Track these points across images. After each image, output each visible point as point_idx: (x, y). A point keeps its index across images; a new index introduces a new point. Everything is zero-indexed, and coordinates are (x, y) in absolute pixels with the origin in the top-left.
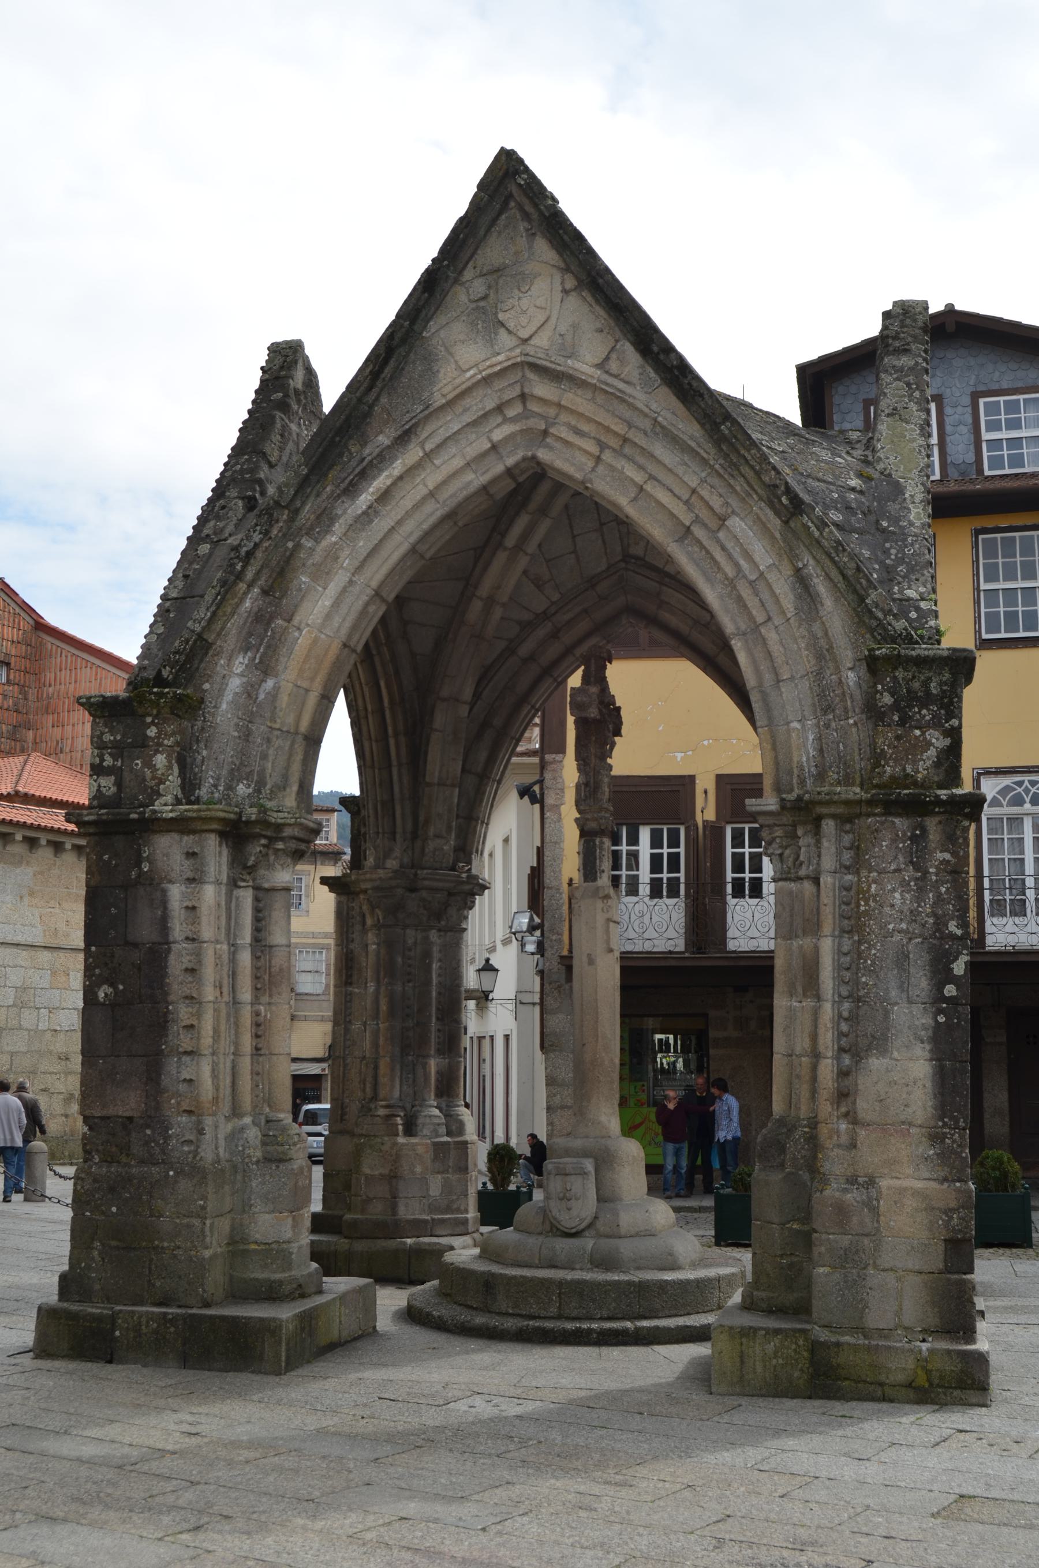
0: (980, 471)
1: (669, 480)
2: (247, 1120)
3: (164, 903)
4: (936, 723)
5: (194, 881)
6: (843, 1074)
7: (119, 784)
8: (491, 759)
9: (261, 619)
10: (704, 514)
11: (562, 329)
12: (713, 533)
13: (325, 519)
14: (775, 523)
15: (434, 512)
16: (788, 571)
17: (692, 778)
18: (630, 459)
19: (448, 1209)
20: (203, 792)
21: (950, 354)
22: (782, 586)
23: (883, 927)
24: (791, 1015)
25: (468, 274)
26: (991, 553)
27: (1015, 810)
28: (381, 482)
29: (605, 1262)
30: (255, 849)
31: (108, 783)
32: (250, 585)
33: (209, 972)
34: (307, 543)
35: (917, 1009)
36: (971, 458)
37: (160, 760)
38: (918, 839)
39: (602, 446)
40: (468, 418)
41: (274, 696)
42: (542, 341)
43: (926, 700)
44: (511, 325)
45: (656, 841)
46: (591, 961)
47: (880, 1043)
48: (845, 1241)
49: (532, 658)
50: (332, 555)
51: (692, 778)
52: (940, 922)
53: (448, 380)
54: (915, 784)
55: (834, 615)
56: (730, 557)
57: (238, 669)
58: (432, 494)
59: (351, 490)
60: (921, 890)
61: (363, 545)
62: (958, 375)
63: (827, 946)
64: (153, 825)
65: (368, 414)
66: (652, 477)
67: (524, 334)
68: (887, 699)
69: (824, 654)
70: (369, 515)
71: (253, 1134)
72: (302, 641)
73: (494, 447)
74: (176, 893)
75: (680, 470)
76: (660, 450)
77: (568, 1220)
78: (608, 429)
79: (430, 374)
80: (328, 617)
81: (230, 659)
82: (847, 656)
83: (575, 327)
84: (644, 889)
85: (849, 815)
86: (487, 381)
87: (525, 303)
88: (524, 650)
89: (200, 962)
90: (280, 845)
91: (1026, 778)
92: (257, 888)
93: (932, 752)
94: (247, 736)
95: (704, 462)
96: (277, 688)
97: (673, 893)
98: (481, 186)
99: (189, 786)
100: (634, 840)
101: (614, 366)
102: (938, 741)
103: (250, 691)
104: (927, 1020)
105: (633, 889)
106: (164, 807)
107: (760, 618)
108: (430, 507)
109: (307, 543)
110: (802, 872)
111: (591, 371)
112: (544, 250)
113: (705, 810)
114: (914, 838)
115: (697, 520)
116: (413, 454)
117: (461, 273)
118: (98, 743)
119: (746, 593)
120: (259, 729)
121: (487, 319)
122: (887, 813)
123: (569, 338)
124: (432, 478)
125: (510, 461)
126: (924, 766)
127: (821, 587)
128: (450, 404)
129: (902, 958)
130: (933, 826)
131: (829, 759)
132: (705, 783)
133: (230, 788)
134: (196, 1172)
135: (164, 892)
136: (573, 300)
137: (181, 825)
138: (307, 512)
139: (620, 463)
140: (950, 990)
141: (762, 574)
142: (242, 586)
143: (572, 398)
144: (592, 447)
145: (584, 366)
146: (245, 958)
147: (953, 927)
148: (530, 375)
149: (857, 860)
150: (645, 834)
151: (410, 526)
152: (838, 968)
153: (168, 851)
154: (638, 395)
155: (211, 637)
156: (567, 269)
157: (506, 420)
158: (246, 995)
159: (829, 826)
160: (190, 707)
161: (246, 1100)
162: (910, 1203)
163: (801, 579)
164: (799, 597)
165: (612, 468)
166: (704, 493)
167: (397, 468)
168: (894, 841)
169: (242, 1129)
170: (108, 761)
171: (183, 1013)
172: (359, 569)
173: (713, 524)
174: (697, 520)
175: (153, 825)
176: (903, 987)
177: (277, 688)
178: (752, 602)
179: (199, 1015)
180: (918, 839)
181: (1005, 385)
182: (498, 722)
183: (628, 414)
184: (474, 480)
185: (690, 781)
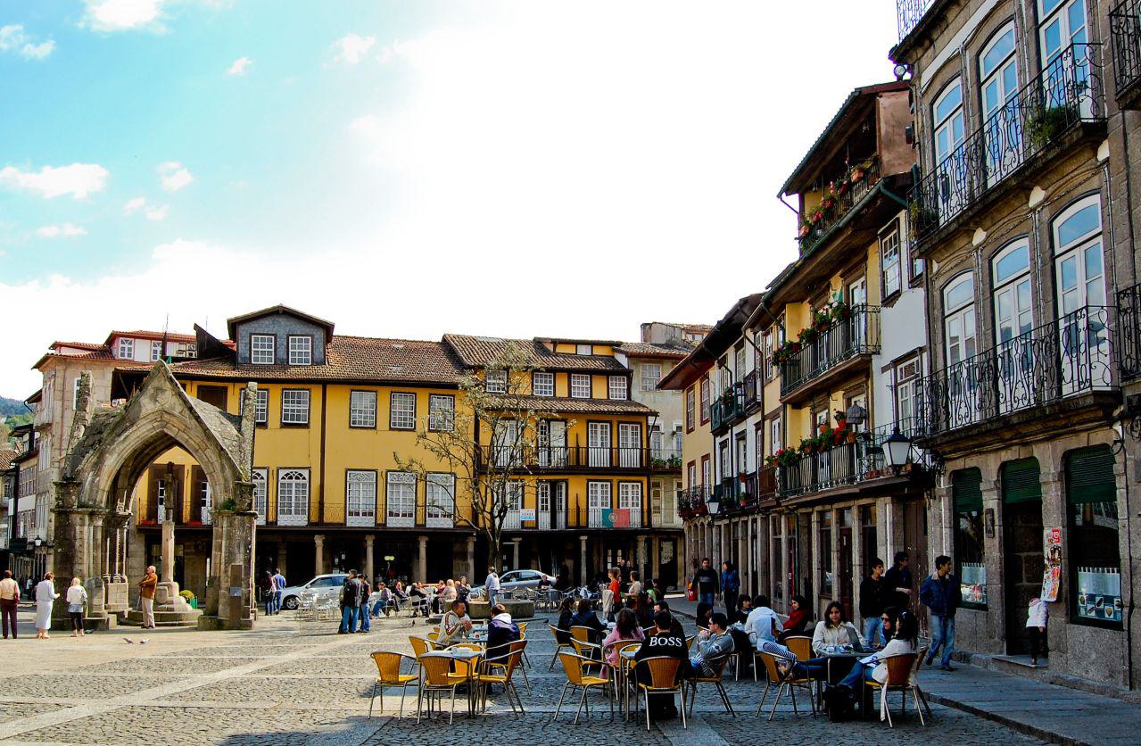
0: (288, 362)
8: (135, 481)
13: (113, 441)
21: (280, 320)
22: (217, 465)
24: (216, 555)
25: (150, 388)
27: (290, 481)
28: (126, 434)
29: (172, 610)
33: (86, 545)
36: (285, 357)
37: (74, 497)
42: (166, 406)
49: (148, 454)
53: (144, 412)
55: (228, 472)
59: (119, 435)
62: (283, 326)
63: (224, 542)
69: (226, 480)
71: (93, 582)
74: (78, 527)
88: (146, 452)
91: (294, 471)
116: (135, 428)
118: (57, 493)
120: (95, 489)
132: (188, 468)
145: (176, 413)
149: (231, 525)
152: (226, 547)
153: (76, 519)
158: (92, 550)
160: (79, 484)
161: (92, 574)
167: (131, 431)
171: (79, 555)
175: (72, 512)
182: (138, 470)
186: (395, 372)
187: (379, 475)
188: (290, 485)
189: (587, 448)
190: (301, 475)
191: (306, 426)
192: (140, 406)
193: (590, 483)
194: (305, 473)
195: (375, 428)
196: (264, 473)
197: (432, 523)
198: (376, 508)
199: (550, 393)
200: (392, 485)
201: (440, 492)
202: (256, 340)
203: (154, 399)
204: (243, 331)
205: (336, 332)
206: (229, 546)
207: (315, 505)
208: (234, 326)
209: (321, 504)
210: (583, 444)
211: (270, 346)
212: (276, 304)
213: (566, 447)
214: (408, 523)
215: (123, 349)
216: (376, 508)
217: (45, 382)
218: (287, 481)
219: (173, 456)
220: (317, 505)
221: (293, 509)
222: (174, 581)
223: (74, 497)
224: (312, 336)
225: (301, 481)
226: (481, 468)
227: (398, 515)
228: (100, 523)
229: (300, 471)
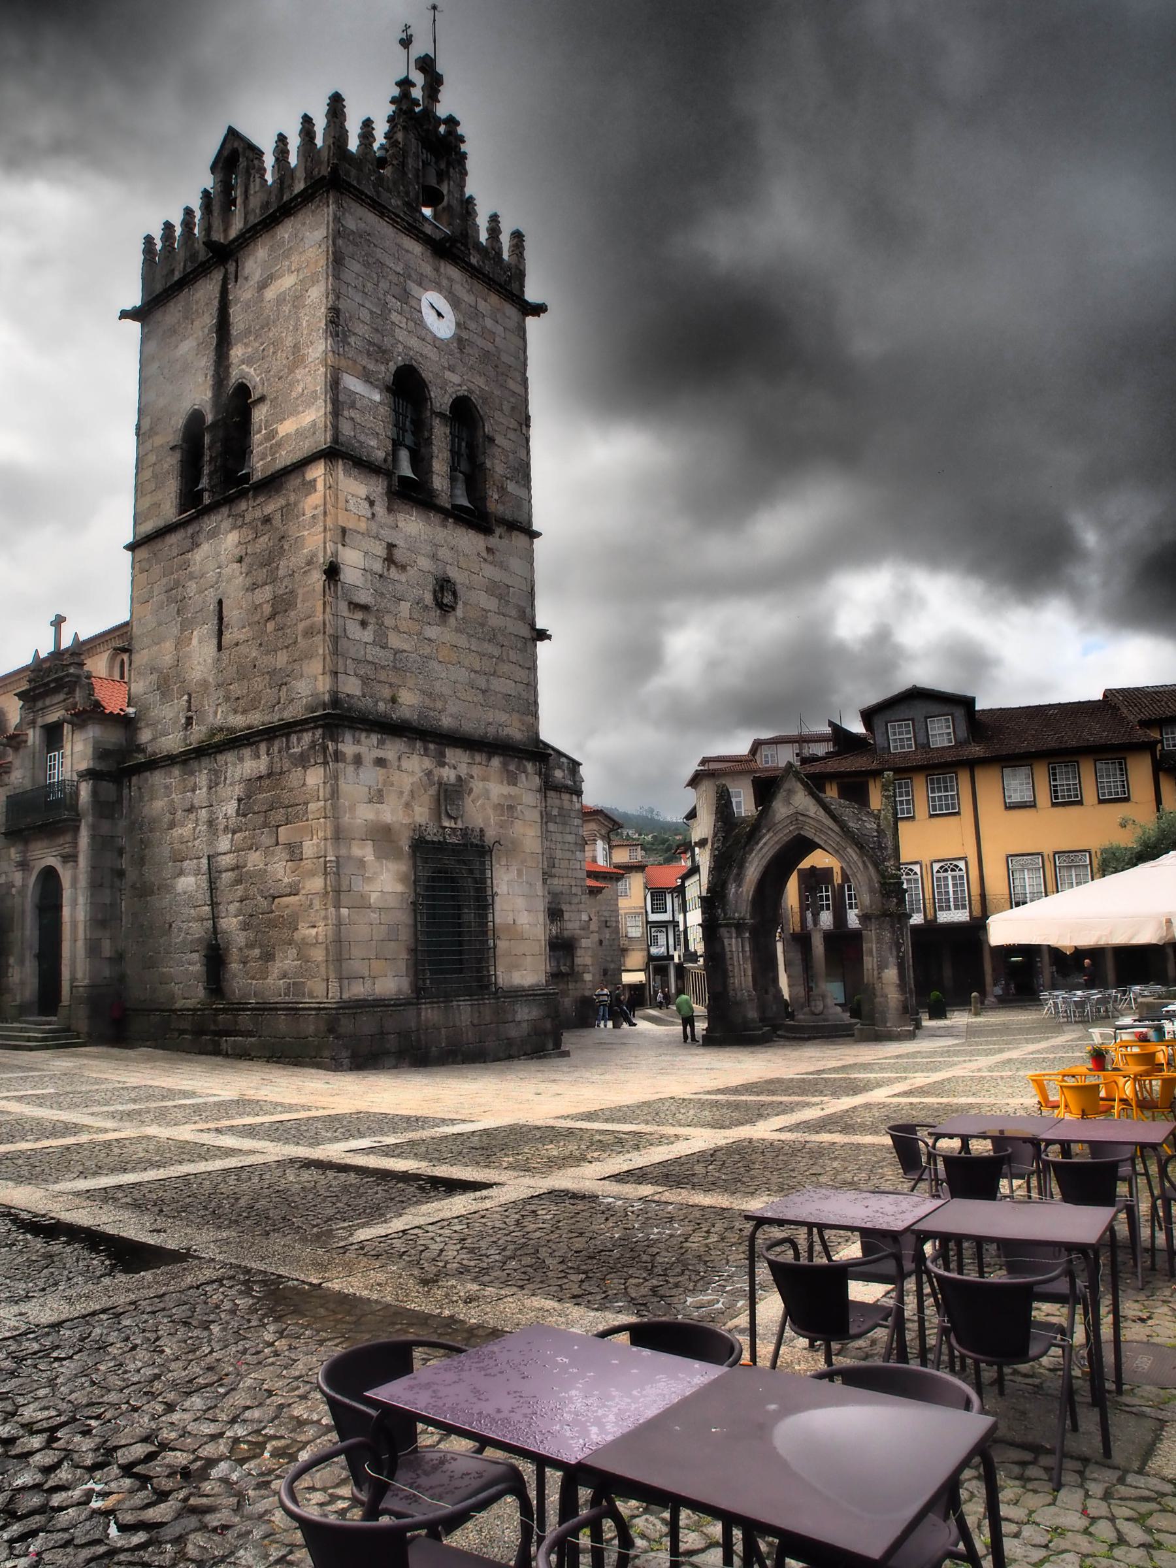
22: (860, 865)
26: (932, 783)
28: (764, 840)
29: (826, 1020)
59: (757, 843)
62: (919, 709)
64: (721, 926)
69: (870, 880)
70: (762, 848)
72: (748, 879)
74: (726, 941)
77: (817, 1012)
85: (877, 918)
97: (828, 909)
103: (737, 891)
121: (788, 802)
132: (837, 870)
137: (726, 925)
143: (808, 820)
153: (723, 931)
154: (824, 820)
163: (864, 862)
167: (767, 837)
171: (730, 968)
175: (721, 926)
186: (1051, 741)
187: (1046, 858)
188: (946, 878)
190: (957, 866)
191: (958, 813)
194: (962, 864)
196: (917, 868)
202: (893, 727)
203: (788, 802)
204: (878, 722)
205: (978, 707)
207: (976, 897)
208: (868, 716)
209: (983, 895)
211: (908, 732)
215: (766, 756)
218: (942, 875)
219: (818, 859)
220: (978, 898)
221: (952, 904)
224: (952, 715)
225: (957, 873)
228: (747, 935)
229: (955, 863)
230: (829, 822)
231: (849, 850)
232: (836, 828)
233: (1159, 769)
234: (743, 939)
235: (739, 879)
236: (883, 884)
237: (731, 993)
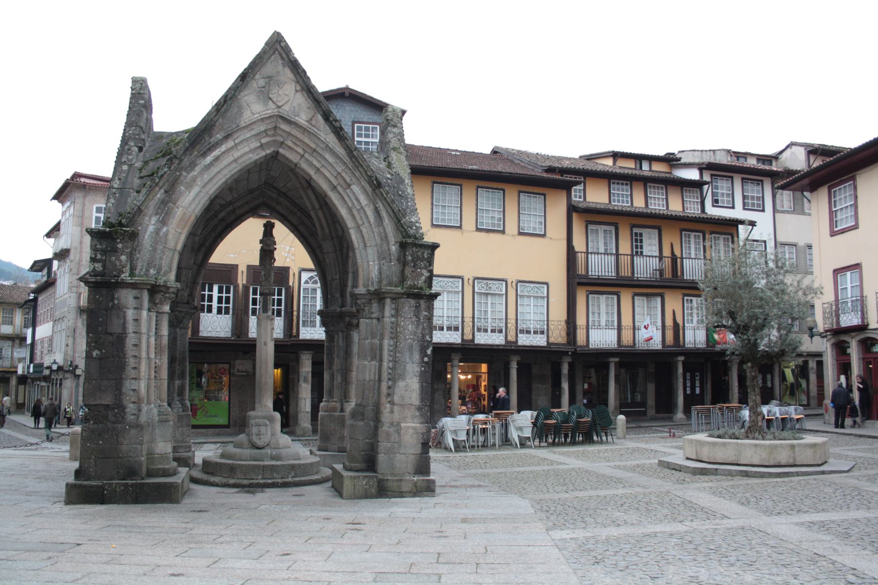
1: (330, 168)
2: (153, 405)
3: (125, 318)
4: (425, 268)
5: (138, 308)
6: (389, 387)
7: (104, 266)
9: (164, 202)
10: (342, 182)
11: (295, 104)
12: (345, 189)
13: (193, 165)
14: (369, 189)
15: (236, 168)
16: (372, 207)
17: (237, 266)
18: (315, 158)
19: (183, 441)
20: (137, 272)
21: (345, 104)
23: (405, 337)
25: (257, 77)
28: (216, 153)
30: (159, 297)
31: (99, 266)
32: (160, 188)
34: (184, 174)
35: (415, 365)
37: (123, 258)
38: (418, 307)
39: (305, 151)
40: (253, 133)
41: (166, 234)
43: (422, 260)
44: (274, 100)
45: (220, 291)
46: (265, 344)
47: (402, 377)
48: (389, 445)
49: (223, 219)
50: (194, 180)
51: (237, 266)
52: (423, 336)
53: (247, 117)
54: (417, 288)
56: (350, 199)
57: (153, 222)
58: (235, 160)
59: (204, 155)
60: (418, 325)
61: (207, 177)
65: (214, 125)
66: (323, 166)
67: (280, 104)
68: (410, 258)
71: (155, 411)
72: (179, 213)
73: (262, 145)
74: (130, 314)
75: (335, 165)
76: (328, 156)
77: (260, 443)
78: (308, 145)
79: (240, 113)
80: (190, 204)
81: (150, 218)
82: (392, 240)
83: (299, 105)
84: (215, 310)
85: (396, 298)
86: (262, 120)
87: (281, 92)
88: (221, 216)
89: (140, 342)
90: (167, 295)
92: (157, 312)
93: (424, 278)
94: (155, 249)
95: (345, 163)
96: (168, 231)
97: (227, 312)
98: (267, 44)
99: (132, 269)
100: (211, 290)
101: (314, 122)
102: (427, 274)
103: (157, 232)
104: (418, 369)
105: (210, 310)
106: (125, 276)
107: (360, 223)
108: (234, 165)
109: (184, 174)
110: (374, 316)
111: (305, 123)
112: (288, 74)
113: (242, 279)
114: (416, 307)
115: (339, 184)
116: (230, 144)
117: (254, 75)
118: (94, 248)
119: (355, 213)
120: (160, 247)
122: (408, 297)
123: (297, 108)
124: (237, 154)
125: (268, 152)
126: (421, 282)
127: (384, 214)
128: (247, 126)
129: (411, 347)
130: (422, 302)
131: (384, 276)
132: (242, 268)
133: (147, 270)
134: (139, 426)
135: (124, 312)
136: (299, 95)
137: (134, 286)
138: (186, 161)
139: (311, 159)
140: (426, 359)
141: (362, 207)
142: (157, 188)
144: (301, 151)
145: (302, 120)
146: (153, 340)
147: (428, 338)
148: (280, 120)
149: (397, 313)
150: (216, 288)
151: (225, 172)
153: (127, 297)
154: (322, 136)
155: (143, 208)
156: (298, 82)
157: (267, 135)
158: (152, 356)
159: (388, 301)
160: (134, 236)
161: (153, 398)
162: (411, 431)
163: (377, 211)
164: (375, 217)
165: (307, 160)
166: (344, 175)
167: (223, 148)
168: (410, 307)
169: (151, 409)
170: (99, 256)
171: (131, 362)
172: (204, 187)
173: (345, 186)
174: (339, 184)
176: (411, 358)
177: (168, 231)
178: (358, 217)
179: (139, 363)
180: (418, 307)
181: (365, 120)
182: (207, 244)
183: (317, 141)
184: (254, 157)
185: (235, 267)
189: (682, 258)
192: (240, 108)
193: (686, 298)
195: (460, 227)
197: (524, 340)
198: (463, 322)
199: (627, 202)
200: (480, 294)
201: (532, 304)
203: (265, 96)
206: (395, 349)
210: (677, 253)
212: (343, 85)
213: (661, 257)
214: (497, 340)
216: (463, 322)
217: (64, 213)
222: (275, 410)
223: (123, 258)
226: (578, 281)
227: (486, 331)
228: (167, 308)
230: (331, 139)
231: (355, 188)
232: (340, 150)
233: (572, 209)
234: (158, 313)
235: (165, 209)
236: (403, 246)
237: (131, 408)
